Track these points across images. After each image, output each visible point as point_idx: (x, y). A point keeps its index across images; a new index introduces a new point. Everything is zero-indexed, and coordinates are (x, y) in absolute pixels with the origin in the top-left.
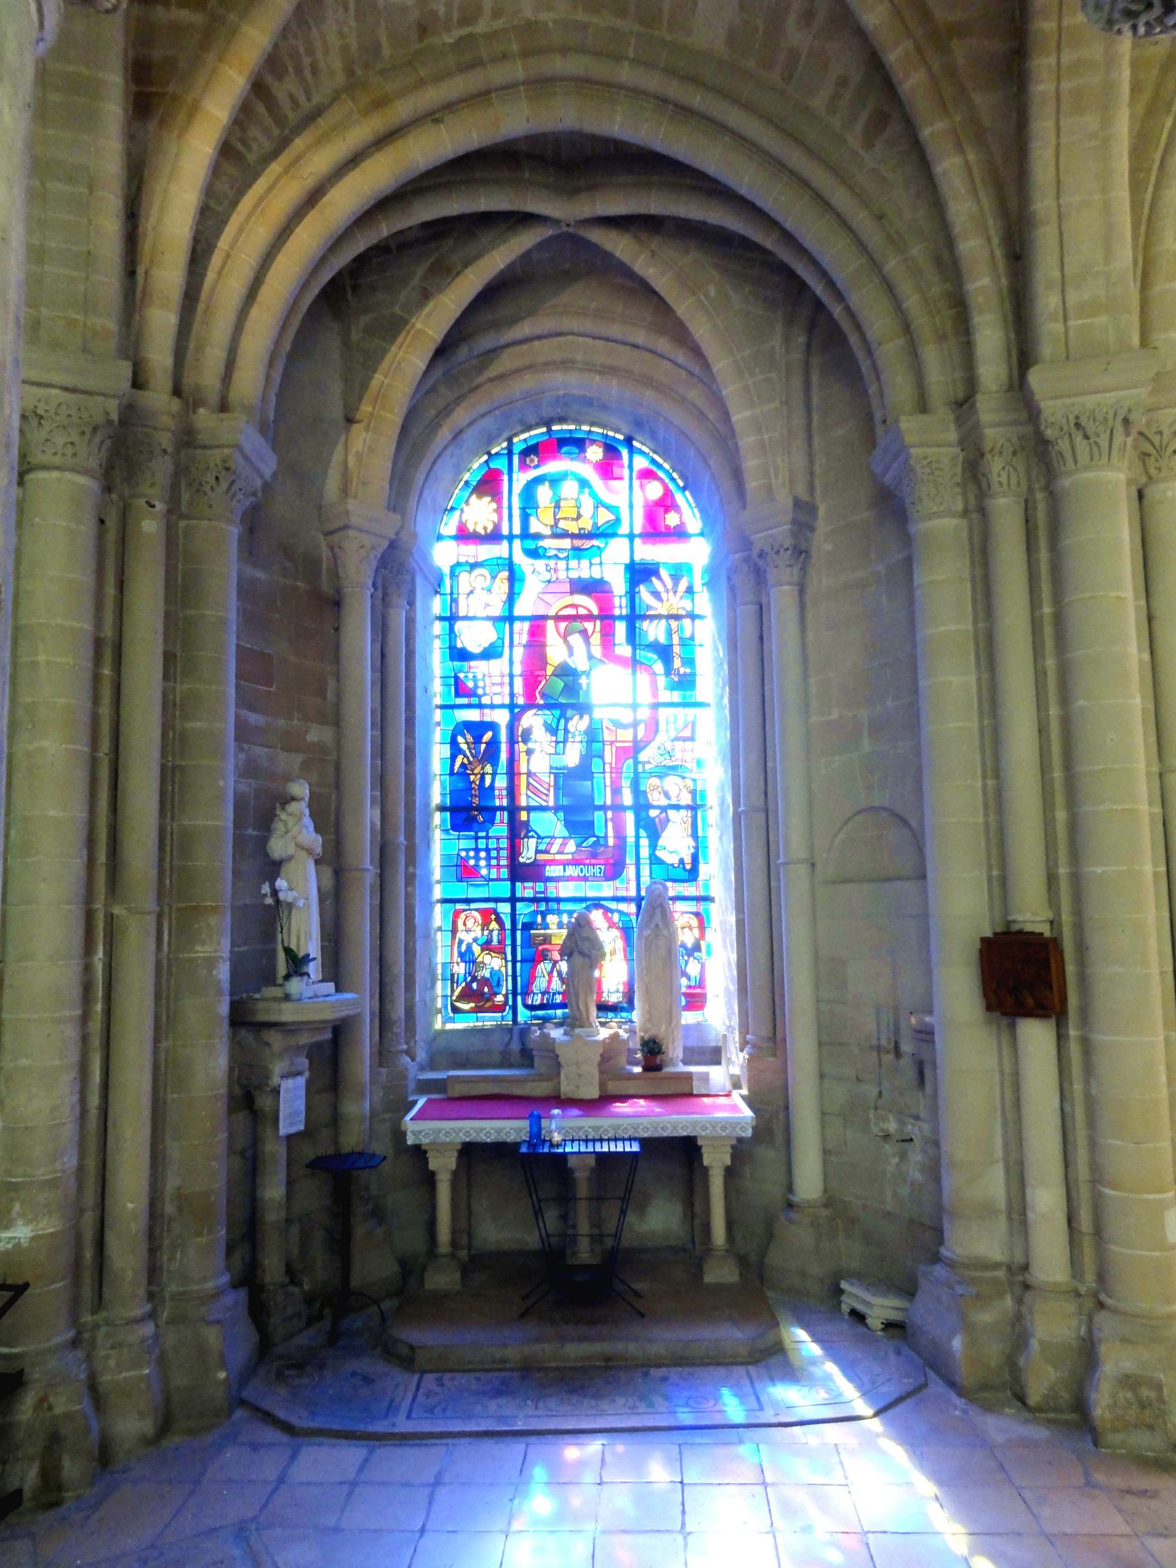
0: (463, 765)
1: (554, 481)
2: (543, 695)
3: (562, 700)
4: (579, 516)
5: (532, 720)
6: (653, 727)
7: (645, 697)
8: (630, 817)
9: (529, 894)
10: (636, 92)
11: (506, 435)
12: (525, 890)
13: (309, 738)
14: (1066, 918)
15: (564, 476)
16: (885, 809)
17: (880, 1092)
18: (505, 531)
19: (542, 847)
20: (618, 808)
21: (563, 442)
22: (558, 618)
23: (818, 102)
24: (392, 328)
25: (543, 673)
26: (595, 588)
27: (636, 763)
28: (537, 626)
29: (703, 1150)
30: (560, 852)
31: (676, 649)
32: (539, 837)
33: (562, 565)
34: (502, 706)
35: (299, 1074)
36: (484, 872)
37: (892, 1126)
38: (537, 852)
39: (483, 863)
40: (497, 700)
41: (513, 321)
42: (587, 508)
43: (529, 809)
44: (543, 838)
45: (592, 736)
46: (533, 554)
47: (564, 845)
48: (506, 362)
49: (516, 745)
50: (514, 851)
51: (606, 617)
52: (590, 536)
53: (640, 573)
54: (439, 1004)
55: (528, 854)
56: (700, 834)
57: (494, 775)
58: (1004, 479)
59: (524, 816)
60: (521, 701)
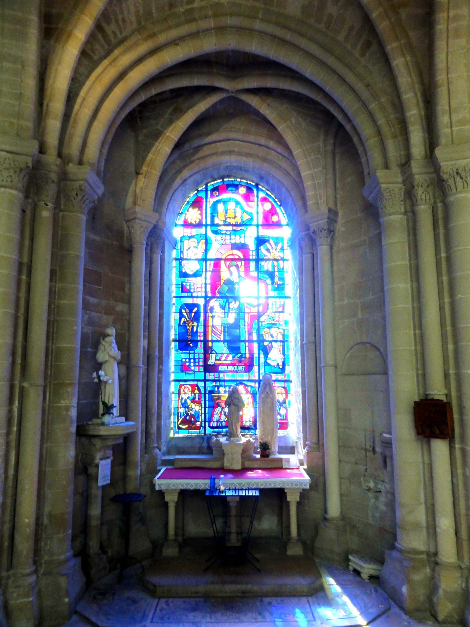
0: (184, 322)
1: (225, 202)
2: (219, 293)
3: (227, 295)
4: (235, 217)
5: (214, 303)
6: (266, 307)
7: (263, 293)
8: (256, 345)
9: (212, 378)
10: (262, 33)
11: (205, 182)
12: (210, 376)
13: (117, 309)
14: (454, 394)
15: (229, 200)
16: (369, 343)
17: (366, 469)
18: (204, 223)
19: (218, 358)
20: (250, 341)
21: (229, 186)
22: (226, 260)
23: (341, 38)
24: (157, 135)
25: (219, 283)
26: (243, 248)
27: (259, 322)
28: (217, 263)
29: (287, 494)
30: (226, 360)
31: (276, 273)
32: (217, 354)
33: (228, 237)
34: (202, 297)
35: (108, 458)
36: (193, 368)
37: (372, 485)
38: (216, 360)
39: (192, 364)
40: (199, 295)
41: (208, 134)
42: (239, 214)
43: (212, 341)
44: (218, 354)
45: (240, 310)
46: (216, 232)
47: (227, 357)
48: (206, 151)
49: (207, 314)
50: (206, 359)
51: (246, 260)
52: (240, 225)
54: (172, 426)
55: (211, 361)
56: (286, 353)
57: (198, 326)
58: (423, 197)
59: (210, 344)
60: (210, 295)
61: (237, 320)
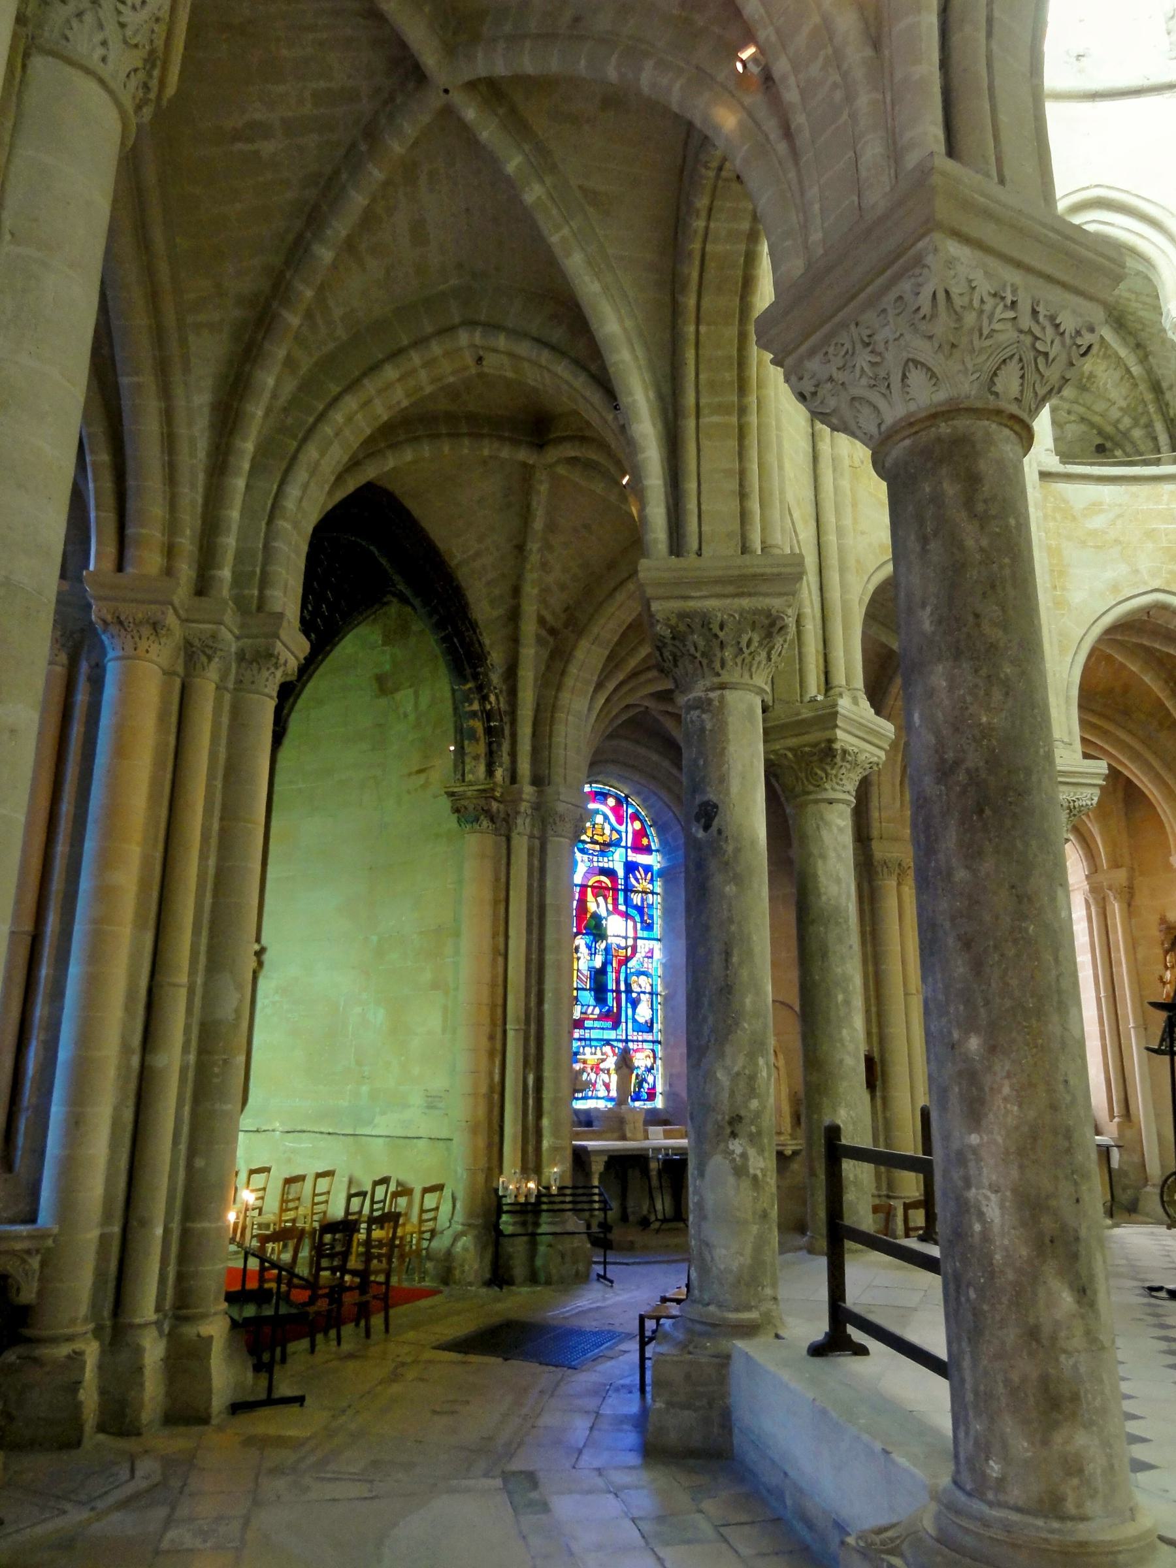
2: (585, 929)
3: (594, 931)
6: (634, 948)
7: (631, 934)
8: (623, 996)
19: (584, 1011)
26: (610, 873)
27: (627, 968)
30: (592, 1014)
31: (646, 910)
33: (595, 859)
38: (582, 1013)
42: (607, 831)
43: (577, 989)
45: (607, 950)
47: (593, 1010)
51: (615, 890)
53: (631, 867)
61: (605, 964)
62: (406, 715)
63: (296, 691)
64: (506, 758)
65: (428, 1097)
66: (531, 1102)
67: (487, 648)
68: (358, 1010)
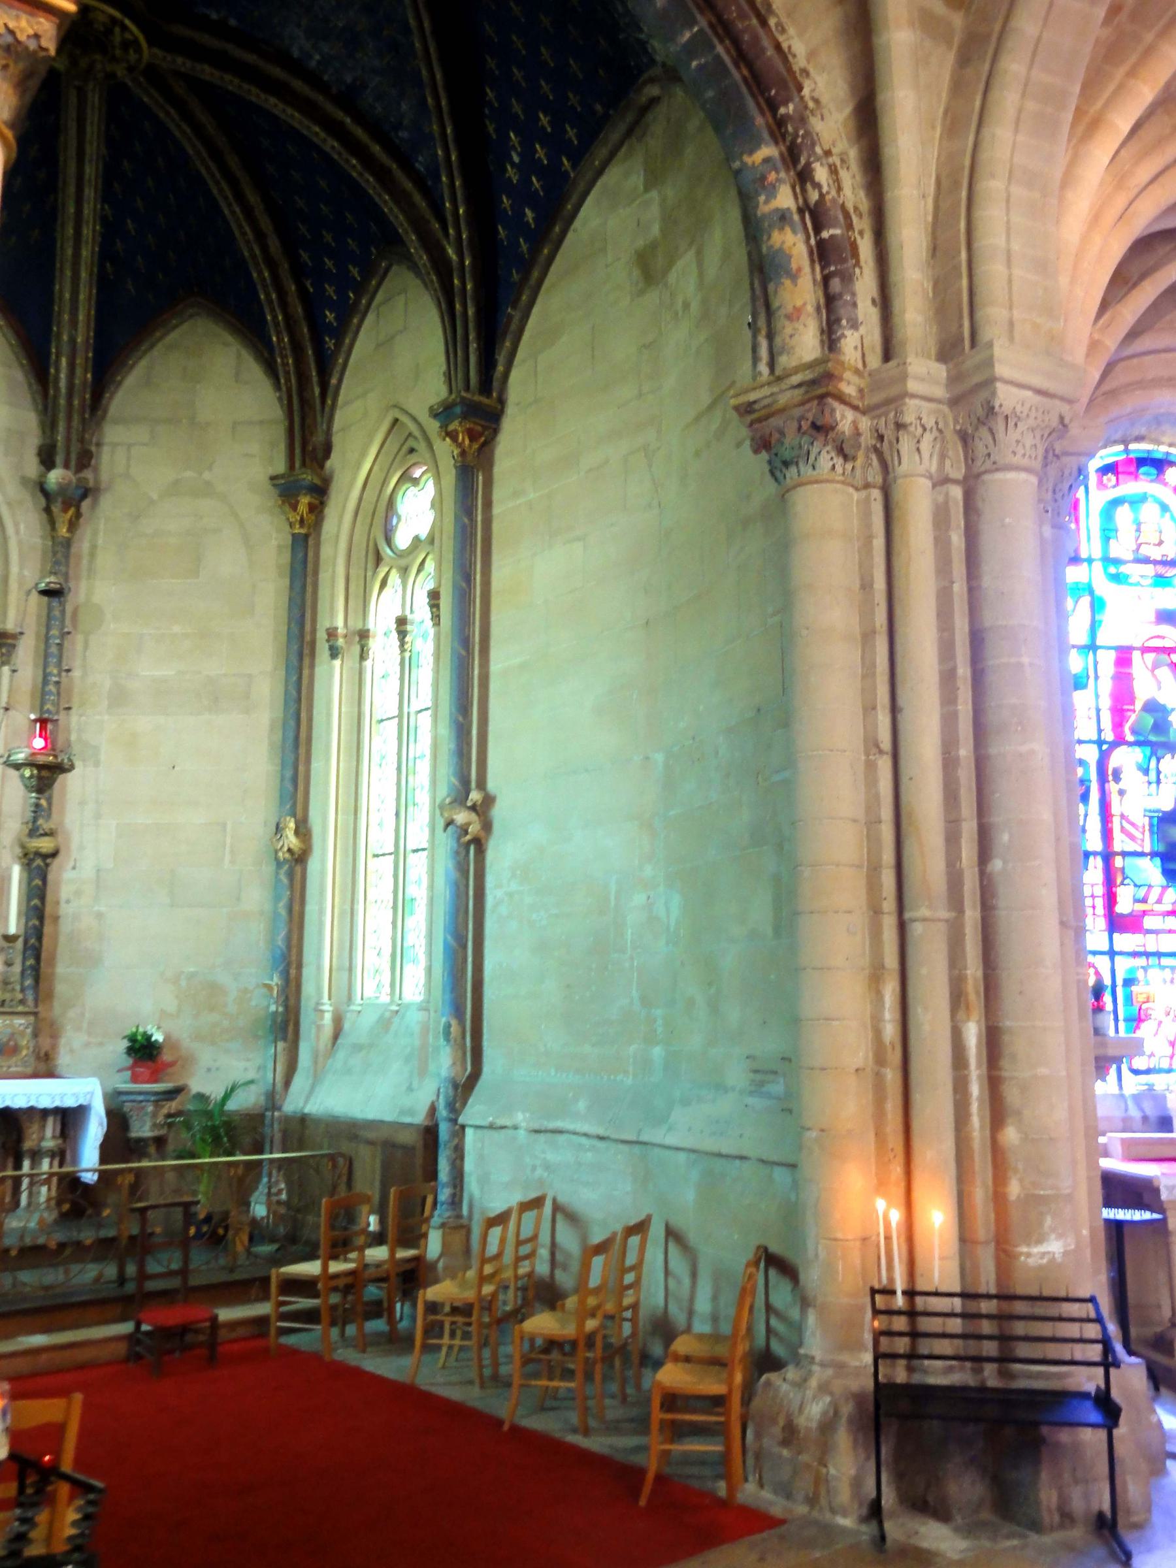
1: (1137, 502)
3: (1153, 738)
4: (1161, 543)
15: (1143, 499)
18: (1084, 554)
21: (1142, 462)
22: (1145, 650)
25: (1132, 707)
28: (1124, 658)
30: (1159, 901)
32: (1135, 885)
43: (1124, 854)
44: (1140, 886)
46: (1116, 578)
49: (1106, 785)
50: (1111, 899)
59: (1118, 862)
60: (1109, 736)
62: (686, 306)
63: (513, 326)
64: (867, 312)
65: (756, 1071)
66: (975, 1089)
67: (800, 61)
68: (639, 899)
